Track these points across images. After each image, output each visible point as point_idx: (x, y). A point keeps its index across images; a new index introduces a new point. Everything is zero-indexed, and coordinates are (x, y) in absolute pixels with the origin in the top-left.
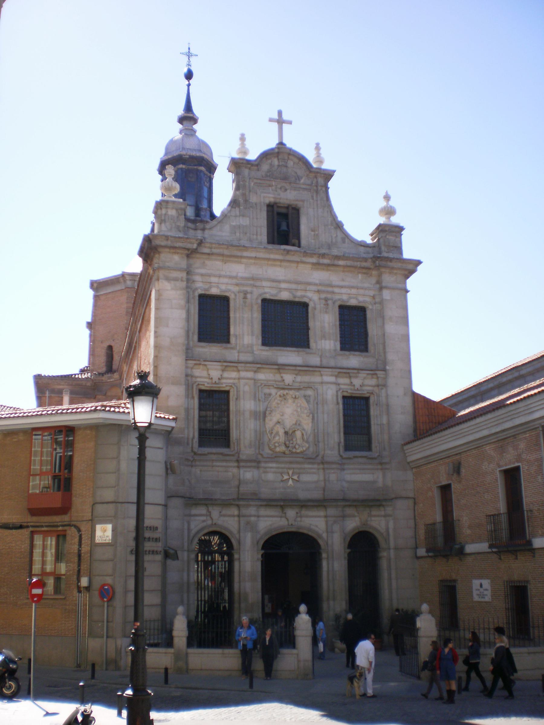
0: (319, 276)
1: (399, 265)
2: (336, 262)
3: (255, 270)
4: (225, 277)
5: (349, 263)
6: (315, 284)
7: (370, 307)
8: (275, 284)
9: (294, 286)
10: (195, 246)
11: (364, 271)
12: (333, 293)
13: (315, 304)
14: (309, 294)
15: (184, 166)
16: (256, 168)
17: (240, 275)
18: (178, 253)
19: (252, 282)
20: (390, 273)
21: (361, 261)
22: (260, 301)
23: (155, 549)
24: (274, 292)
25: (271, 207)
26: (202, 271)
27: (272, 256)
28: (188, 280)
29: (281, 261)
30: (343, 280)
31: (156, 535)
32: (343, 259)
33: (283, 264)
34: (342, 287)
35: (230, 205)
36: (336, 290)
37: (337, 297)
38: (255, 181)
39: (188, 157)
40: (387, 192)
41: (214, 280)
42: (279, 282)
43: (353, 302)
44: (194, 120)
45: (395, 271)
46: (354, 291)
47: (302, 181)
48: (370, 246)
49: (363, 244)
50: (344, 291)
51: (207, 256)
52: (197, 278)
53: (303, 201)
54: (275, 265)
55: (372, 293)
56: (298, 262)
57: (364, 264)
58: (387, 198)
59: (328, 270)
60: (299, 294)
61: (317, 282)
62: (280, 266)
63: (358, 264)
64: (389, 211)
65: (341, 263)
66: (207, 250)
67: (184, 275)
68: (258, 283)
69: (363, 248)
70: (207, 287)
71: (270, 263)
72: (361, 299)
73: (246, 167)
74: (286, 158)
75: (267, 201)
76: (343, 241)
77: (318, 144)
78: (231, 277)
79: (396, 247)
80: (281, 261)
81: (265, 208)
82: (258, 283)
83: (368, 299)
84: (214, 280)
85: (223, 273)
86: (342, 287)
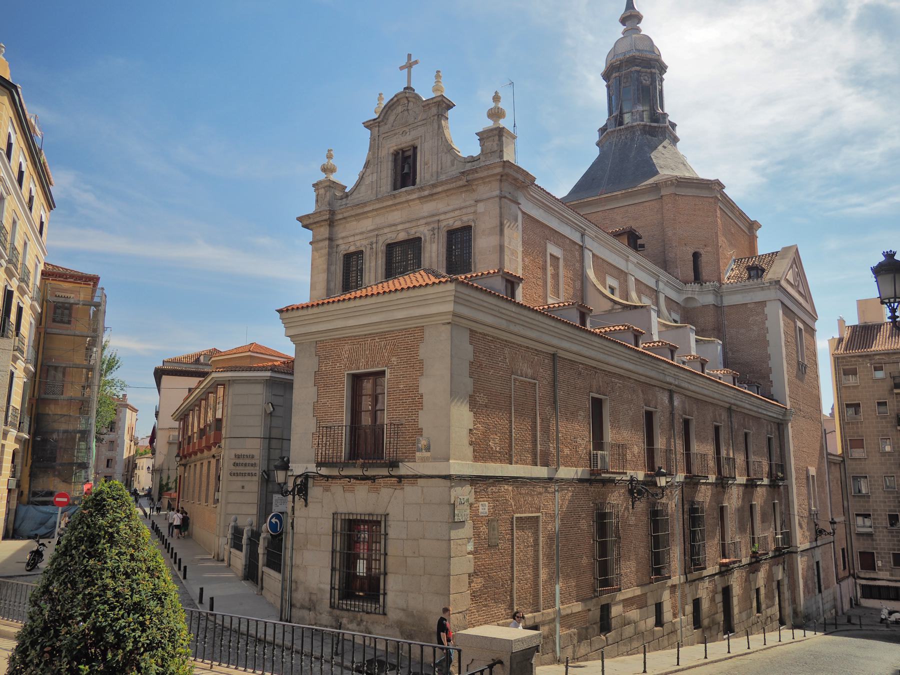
0: (428, 208)
1: (485, 173)
2: (435, 191)
3: (380, 220)
4: (357, 234)
5: (445, 187)
6: (424, 218)
7: (473, 225)
8: (393, 228)
9: (407, 225)
10: (327, 217)
11: (464, 189)
12: (439, 221)
13: (425, 236)
14: (421, 229)
15: (617, 74)
16: (383, 123)
17: (369, 228)
18: (323, 226)
19: (376, 233)
20: (484, 183)
21: (456, 182)
22: (384, 248)
23: (252, 471)
24: (394, 235)
25: (396, 154)
26: (343, 235)
27: (385, 204)
28: (330, 247)
29: (395, 205)
30: (448, 205)
31: (253, 462)
32: (441, 186)
33: (398, 207)
34: (445, 213)
35: (364, 167)
36: (442, 217)
37: (444, 223)
38: (383, 136)
39: (619, 62)
40: (496, 93)
41: (351, 239)
42: (394, 225)
43: (458, 224)
44: (638, 18)
45: (487, 180)
46: (457, 213)
47: (420, 118)
48: (476, 159)
49: (472, 160)
50: (448, 216)
51: (344, 221)
52: (340, 242)
53: (418, 138)
54: (393, 211)
55: (472, 210)
56: (407, 201)
57: (461, 183)
58: (496, 98)
59: (434, 200)
60: (413, 231)
61: (426, 214)
62: (397, 210)
63: (452, 186)
64: (496, 114)
65: (440, 189)
66: (340, 216)
67: (327, 243)
68: (381, 232)
69: (470, 164)
70: (347, 248)
71: (388, 210)
72: (465, 218)
73: (376, 127)
74: (406, 102)
75: (391, 151)
76: (453, 165)
77: (438, 72)
78: (362, 233)
79: (493, 152)
80: (395, 205)
81: (391, 158)
82: (381, 232)
83: (471, 217)
84: (351, 239)
85: (357, 231)
86: (445, 213)
